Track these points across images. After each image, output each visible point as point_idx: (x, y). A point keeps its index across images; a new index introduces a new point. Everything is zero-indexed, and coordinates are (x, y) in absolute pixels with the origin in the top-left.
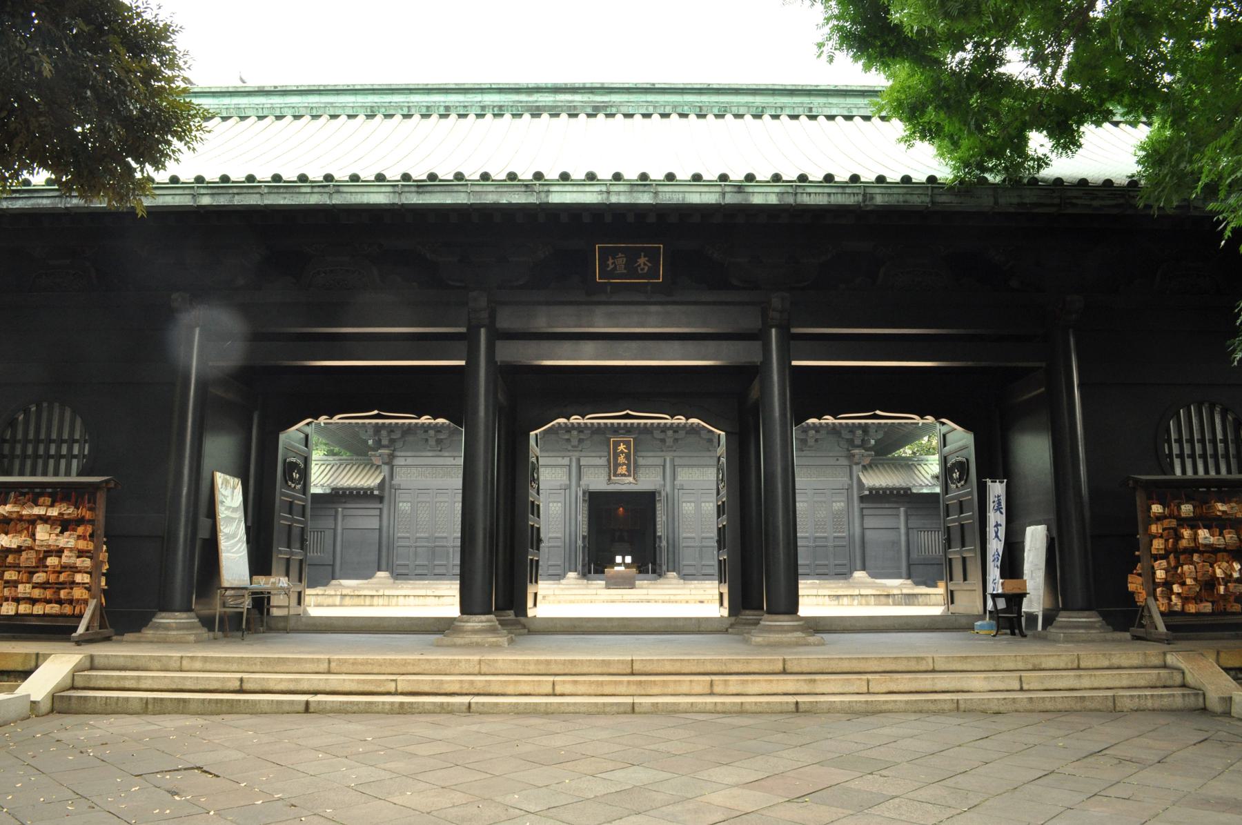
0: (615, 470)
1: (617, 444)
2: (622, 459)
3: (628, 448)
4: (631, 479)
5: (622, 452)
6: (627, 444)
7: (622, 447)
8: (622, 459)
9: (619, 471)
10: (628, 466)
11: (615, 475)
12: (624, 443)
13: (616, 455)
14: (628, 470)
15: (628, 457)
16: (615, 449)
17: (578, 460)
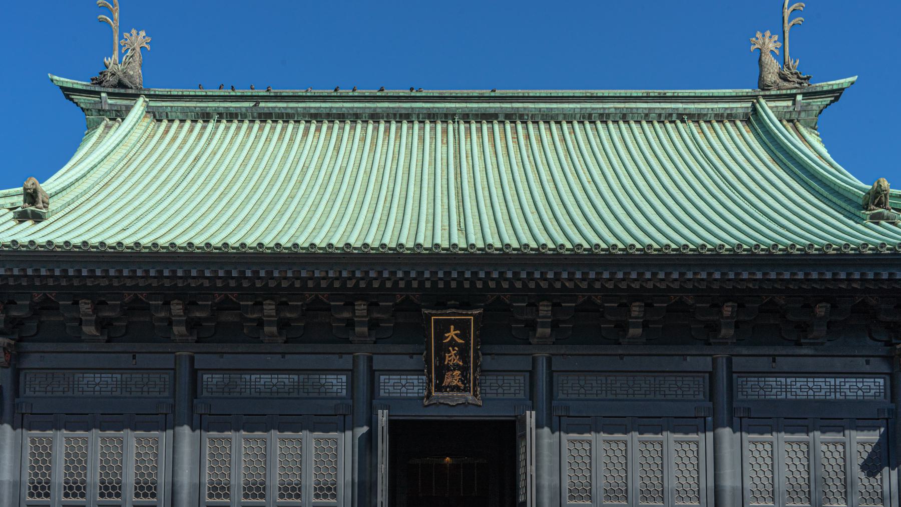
0: (440, 377)
1: (443, 327)
2: (451, 357)
3: (464, 335)
4: (470, 397)
5: (453, 343)
6: (463, 327)
7: (452, 333)
8: (451, 357)
9: (447, 381)
10: (464, 370)
11: (439, 388)
12: (459, 325)
13: (442, 349)
14: (465, 378)
15: (463, 353)
16: (440, 336)
17: (370, 360)
